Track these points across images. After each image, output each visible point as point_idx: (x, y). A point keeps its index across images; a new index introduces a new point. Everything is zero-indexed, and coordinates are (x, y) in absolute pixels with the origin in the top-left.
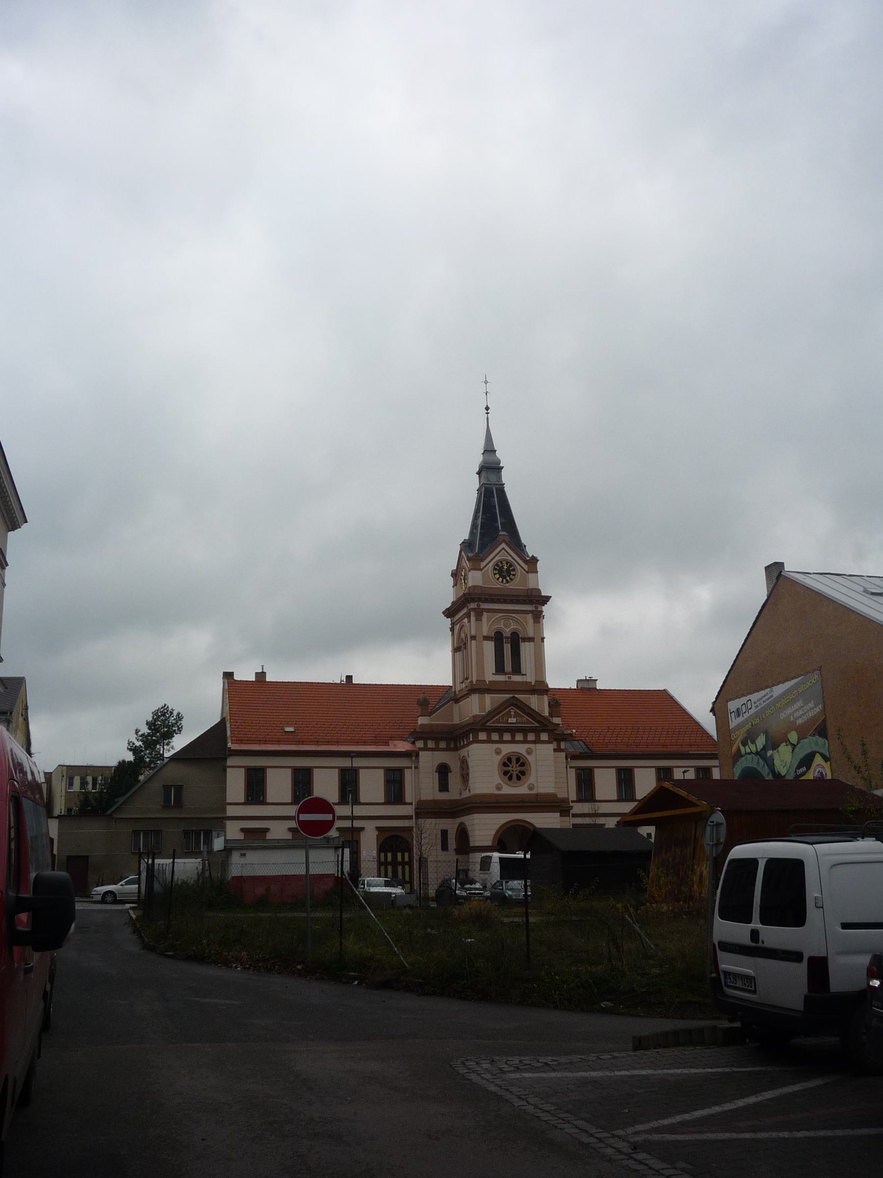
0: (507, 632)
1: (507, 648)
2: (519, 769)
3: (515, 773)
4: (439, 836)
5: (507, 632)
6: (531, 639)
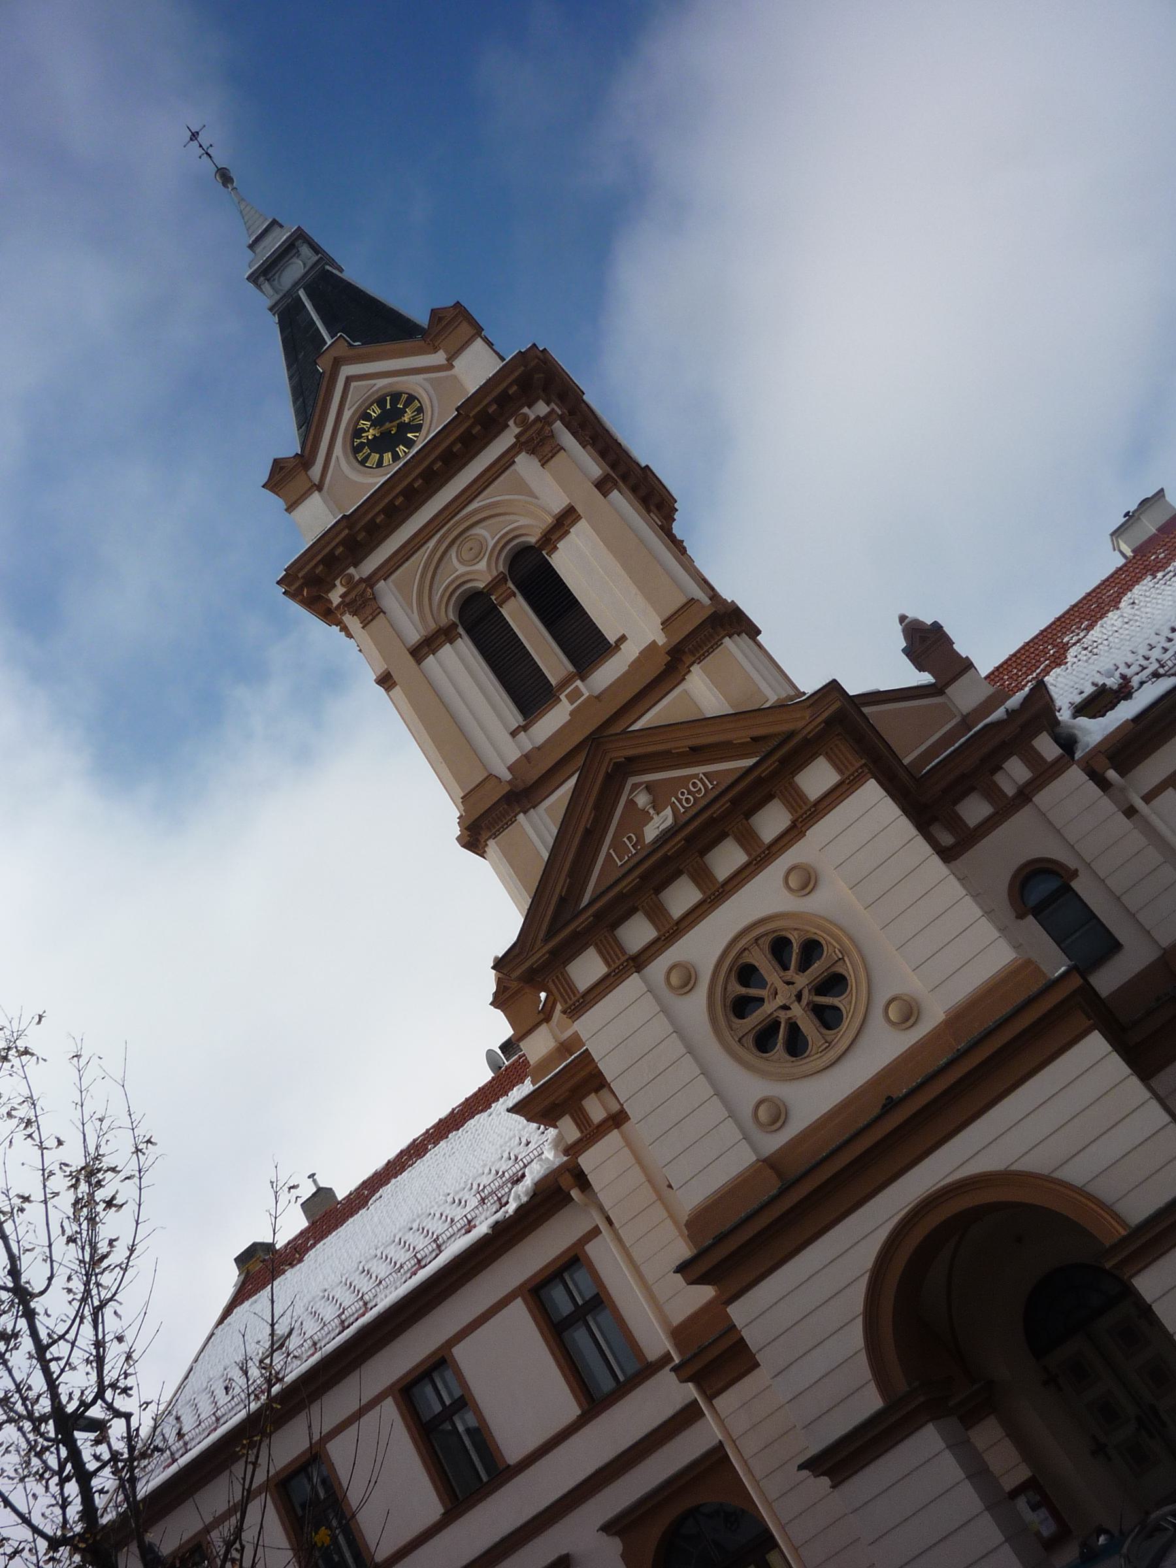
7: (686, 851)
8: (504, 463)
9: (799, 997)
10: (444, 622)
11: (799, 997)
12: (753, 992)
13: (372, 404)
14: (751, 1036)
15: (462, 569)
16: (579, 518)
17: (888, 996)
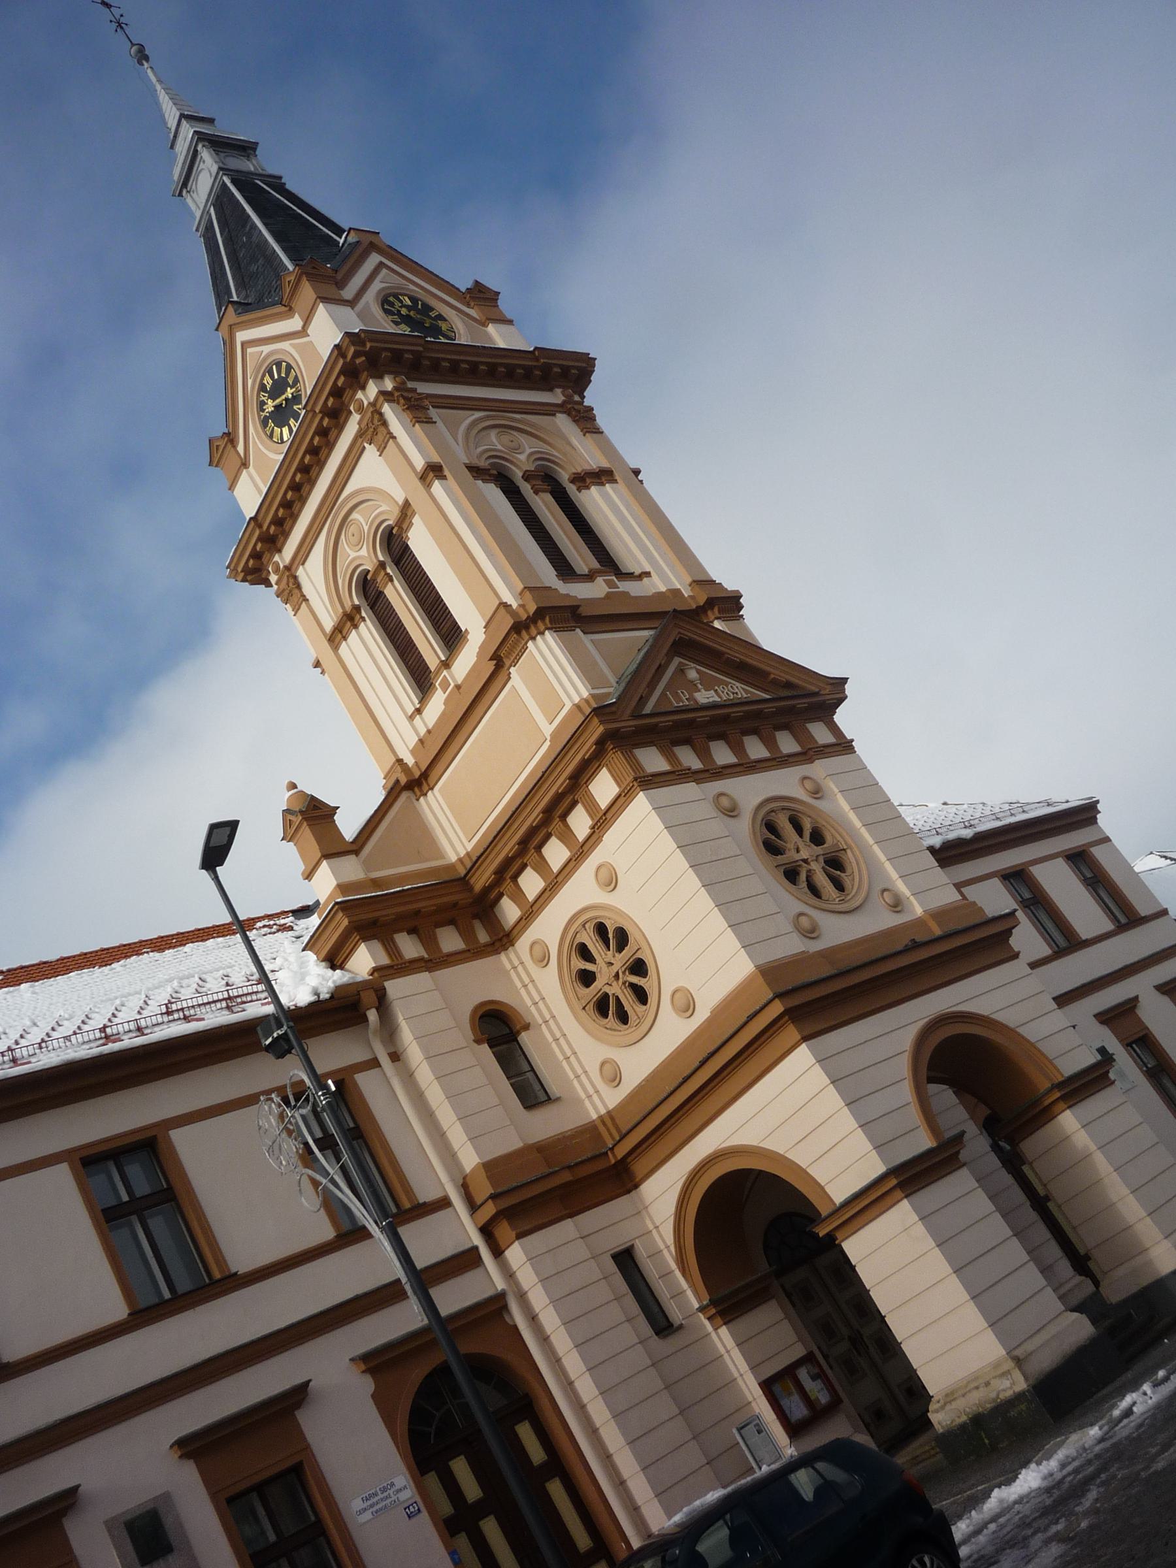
0: (521, 463)
2: (819, 850)
3: (817, 867)
4: (618, 1279)
5: (521, 463)
6: (602, 476)
10: (348, 606)
12: (589, 966)
13: (263, 376)
14: (592, 1004)
15: (353, 555)
16: (414, 513)
17: (673, 988)
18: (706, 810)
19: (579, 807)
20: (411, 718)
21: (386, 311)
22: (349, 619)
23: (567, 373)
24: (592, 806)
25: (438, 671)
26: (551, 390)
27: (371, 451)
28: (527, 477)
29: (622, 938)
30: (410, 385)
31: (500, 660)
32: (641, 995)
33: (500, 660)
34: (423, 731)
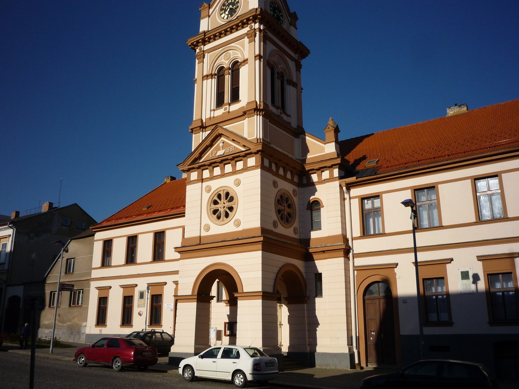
1: (278, 83)
6: (295, 85)
7: (223, 161)
8: (241, 37)
9: (224, 207)
11: (224, 207)
12: (218, 200)
15: (223, 61)
16: (247, 63)
18: (271, 183)
19: (242, 162)
20: (211, 111)
21: (271, 6)
22: (212, 76)
23: (302, 51)
24: (245, 164)
25: (226, 105)
26: (296, 54)
27: (246, 40)
28: (278, 73)
29: (232, 199)
30: (266, 31)
31: (245, 114)
32: (227, 215)
33: (245, 114)
34: (212, 116)
